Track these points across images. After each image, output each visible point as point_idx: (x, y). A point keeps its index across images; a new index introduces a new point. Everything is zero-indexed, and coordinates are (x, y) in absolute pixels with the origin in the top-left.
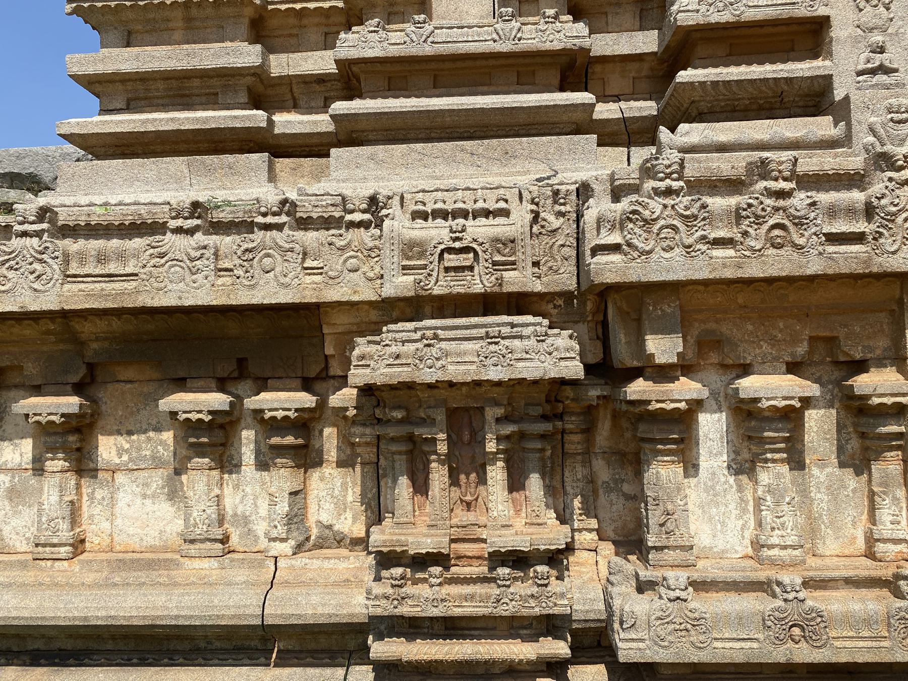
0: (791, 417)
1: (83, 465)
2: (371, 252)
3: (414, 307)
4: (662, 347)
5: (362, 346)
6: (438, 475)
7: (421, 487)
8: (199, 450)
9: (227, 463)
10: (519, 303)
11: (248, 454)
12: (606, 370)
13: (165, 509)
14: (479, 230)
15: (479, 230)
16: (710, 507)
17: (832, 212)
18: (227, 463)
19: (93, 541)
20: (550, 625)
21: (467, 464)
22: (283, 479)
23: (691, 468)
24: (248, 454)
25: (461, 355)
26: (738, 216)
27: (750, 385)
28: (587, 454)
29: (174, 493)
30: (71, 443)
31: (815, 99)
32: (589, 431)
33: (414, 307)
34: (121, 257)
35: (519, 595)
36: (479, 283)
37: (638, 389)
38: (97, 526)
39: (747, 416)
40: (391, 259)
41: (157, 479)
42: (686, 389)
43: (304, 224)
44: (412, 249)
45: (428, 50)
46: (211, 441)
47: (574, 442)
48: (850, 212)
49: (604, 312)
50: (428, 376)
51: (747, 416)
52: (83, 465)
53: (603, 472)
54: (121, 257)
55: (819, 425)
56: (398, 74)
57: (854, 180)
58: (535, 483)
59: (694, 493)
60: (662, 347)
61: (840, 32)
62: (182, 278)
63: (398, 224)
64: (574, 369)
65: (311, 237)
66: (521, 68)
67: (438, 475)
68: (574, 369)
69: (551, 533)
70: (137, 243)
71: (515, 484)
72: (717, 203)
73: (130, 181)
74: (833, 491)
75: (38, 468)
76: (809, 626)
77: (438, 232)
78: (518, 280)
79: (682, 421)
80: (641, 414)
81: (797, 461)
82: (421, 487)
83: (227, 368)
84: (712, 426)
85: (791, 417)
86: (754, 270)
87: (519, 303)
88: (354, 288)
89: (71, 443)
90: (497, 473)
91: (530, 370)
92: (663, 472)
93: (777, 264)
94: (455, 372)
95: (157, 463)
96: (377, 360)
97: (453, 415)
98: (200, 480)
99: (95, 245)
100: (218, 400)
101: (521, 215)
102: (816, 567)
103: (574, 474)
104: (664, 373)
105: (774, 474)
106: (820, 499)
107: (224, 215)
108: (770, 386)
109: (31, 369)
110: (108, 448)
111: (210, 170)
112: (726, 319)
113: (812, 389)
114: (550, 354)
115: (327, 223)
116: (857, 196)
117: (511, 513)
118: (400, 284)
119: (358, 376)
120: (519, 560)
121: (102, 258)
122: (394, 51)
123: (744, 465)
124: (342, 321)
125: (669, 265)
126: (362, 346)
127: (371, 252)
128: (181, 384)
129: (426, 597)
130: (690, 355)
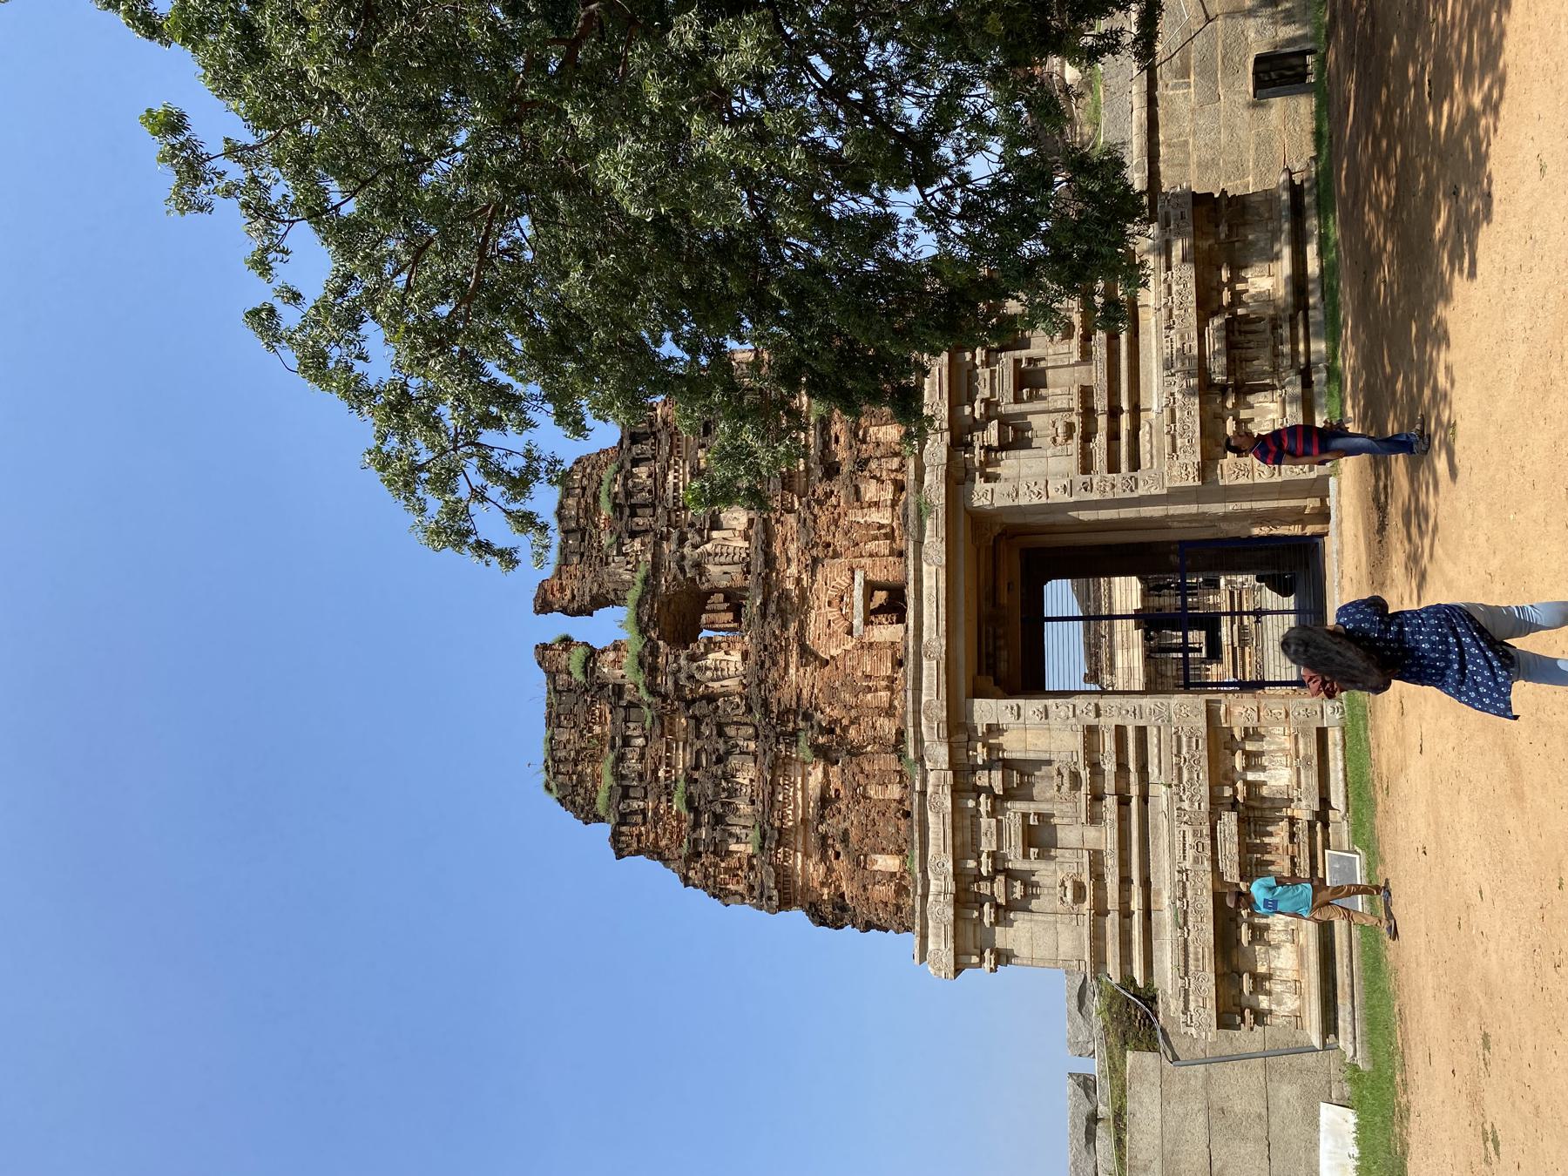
0: (1248, 755)
1: (1268, 977)
2: (1196, 874)
3: (1214, 862)
4: (1228, 792)
5: (1227, 878)
6: (1267, 857)
7: (1272, 863)
8: (1262, 936)
9: (1267, 927)
10: (1213, 829)
12: (1234, 805)
13: (1283, 950)
14: (1190, 840)
15: (1190, 840)
16: (1277, 777)
17: (1189, 746)
18: (1267, 927)
19: (1296, 977)
20: (1311, 826)
21: (1264, 848)
23: (1264, 783)
26: (1190, 772)
27: (1238, 767)
28: (1263, 809)
29: (1278, 947)
30: (1259, 980)
31: (1142, 732)
32: (1253, 808)
33: (1214, 862)
34: (1196, 953)
35: (1303, 837)
36: (1208, 842)
37: (1239, 798)
38: (1291, 975)
39: (1246, 768)
40: (1199, 867)
41: (1272, 953)
42: (1239, 785)
43: (1184, 895)
44: (1196, 860)
46: (1259, 933)
47: (1257, 813)
48: (1189, 741)
49: (1217, 805)
50: (1237, 858)
51: (1246, 768)
52: (1268, 977)
53: (1267, 805)
54: (1196, 953)
55: (1249, 747)
56: (1124, 863)
57: (1179, 738)
59: (1271, 782)
60: (1228, 792)
61: (1120, 723)
62: (1203, 933)
63: (1188, 864)
64: (1234, 815)
65: (1189, 893)
66: (1123, 819)
67: (1267, 857)
68: (1234, 815)
69: (1284, 824)
70: (1191, 949)
71: (1271, 834)
73: (1162, 962)
75: (1269, 993)
76: (1307, 759)
77: (1190, 853)
78: (1206, 830)
79: (1247, 783)
80: (1248, 797)
81: (1261, 754)
82: (1272, 863)
83: (1233, 925)
84: (1251, 776)
85: (1248, 755)
87: (1213, 829)
88: (1208, 879)
89: (1259, 980)
90: (1267, 840)
91: (1235, 829)
92: (1265, 792)
93: (1204, 763)
94: (1235, 850)
95: (1267, 952)
96: (1231, 873)
98: (1272, 937)
99: (1191, 962)
100: (1244, 928)
101: (1185, 827)
102: (1293, 752)
103: (1267, 814)
104: (1235, 791)
105: (1265, 761)
106: (1273, 747)
107: (1181, 921)
108: (1239, 761)
109: (1234, 992)
110: (1262, 969)
111: (1158, 933)
112: (1220, 775)
113: (1239, 753)
115: (1184, 888)
116: (1184, 739)
117: (1278, 836)
118: (1207, 865)
119: (1236, 879)
120: (1292, 836)
121: (1197, 960)
123: (1264, 769)
124: (1218, 886)
125: (1205, 790)
126: (1227, 878)
127: (1196, 874)
128: (1239, 941)
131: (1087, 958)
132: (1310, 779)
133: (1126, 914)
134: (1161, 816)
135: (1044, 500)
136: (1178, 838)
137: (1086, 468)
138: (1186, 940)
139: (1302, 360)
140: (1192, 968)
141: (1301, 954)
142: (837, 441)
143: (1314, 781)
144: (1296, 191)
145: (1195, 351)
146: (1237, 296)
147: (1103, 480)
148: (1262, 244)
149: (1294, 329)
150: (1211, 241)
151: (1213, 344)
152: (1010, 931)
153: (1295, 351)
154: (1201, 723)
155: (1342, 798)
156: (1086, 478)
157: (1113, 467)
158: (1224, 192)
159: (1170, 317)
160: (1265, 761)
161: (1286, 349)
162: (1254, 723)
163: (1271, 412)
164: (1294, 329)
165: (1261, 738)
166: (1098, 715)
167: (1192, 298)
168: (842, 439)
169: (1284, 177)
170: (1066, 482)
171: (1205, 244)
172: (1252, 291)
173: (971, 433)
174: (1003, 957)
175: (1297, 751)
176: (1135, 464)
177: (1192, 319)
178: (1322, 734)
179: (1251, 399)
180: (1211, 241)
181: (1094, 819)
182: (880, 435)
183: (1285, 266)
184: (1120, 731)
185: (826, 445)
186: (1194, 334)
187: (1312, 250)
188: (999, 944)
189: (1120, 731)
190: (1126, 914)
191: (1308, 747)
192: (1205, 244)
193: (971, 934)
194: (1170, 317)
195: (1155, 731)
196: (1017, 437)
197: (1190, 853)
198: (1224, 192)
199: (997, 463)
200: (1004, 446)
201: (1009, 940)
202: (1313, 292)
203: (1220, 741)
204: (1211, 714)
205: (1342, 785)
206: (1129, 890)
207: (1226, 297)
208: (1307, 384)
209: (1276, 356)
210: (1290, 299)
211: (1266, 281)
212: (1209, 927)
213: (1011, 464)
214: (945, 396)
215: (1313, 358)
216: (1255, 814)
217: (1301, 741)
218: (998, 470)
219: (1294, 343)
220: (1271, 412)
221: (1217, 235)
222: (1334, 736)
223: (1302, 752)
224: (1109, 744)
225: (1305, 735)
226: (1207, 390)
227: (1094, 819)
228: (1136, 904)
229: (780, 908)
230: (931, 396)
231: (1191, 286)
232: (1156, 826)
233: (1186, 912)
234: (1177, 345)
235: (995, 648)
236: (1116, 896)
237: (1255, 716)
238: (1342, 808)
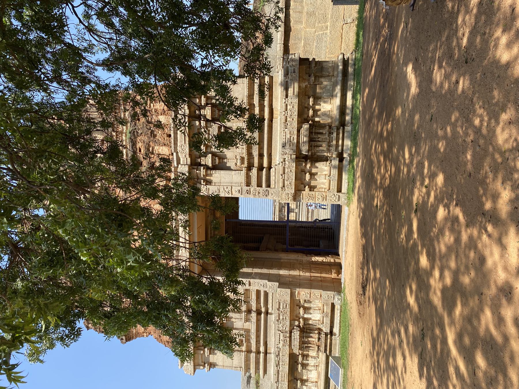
1: (307, 381)
4: (297, 323)
6: (309, 345)
9: (307, 365)
11: (307, 362)
14: (282, 338)
15: (282, 338)
16: (315, 317)
18: (307, 365)
22: (310, 359)
23: (310, 319)
24: (307, 362)
25: (296, 343)
29: (311, 371)
36: (288, 339)
42: (301, 320)
44: (283, 345)
45: (255, 334)
48: (283, 305)
52: (307, 381)
54: (282, 375)
55: (306, 305)
56: (258, 337)
57: (279, 303)
58: (311, 335)
62: (285, 369)
63: (280, 346)
65: (281, 354)
66: (258, 321)
70: (280, 373)
71: (311, 337)
72: (281, 318)
74: (314, 304)
77: (282, 342)
78: (288, 335)
79: (305, 320)
83: (296, 364)
84: (306, 316)
86: (289, 315)
90: (310, 339)
92: (310, 322)
93: (288, 313)
94: (298, 344)
95: (307, 372)
97: (303, 344)
99: (280, 377)
100: (300, 365)
106: (315, 306)
109: (294, 385)
110: (305, 378)
111: (269, 361)
112: (294, 317)
114: (296, 334)
116: (281, 304)
117: (314, 338)
118: (287, 347)
120: (319, 339)
122: (255, 338)
123: (311, 314)
125: (288, 323)
128: (297, 369)
129: (322, 348)
130: (297, 319)
131: (243, 367)
132: (327, 321)
133: (258, 352)
134: (272, 323)
135: (230, 196)
136: (278, 337)
137: (248, 184)
138: (278, 371)
139: (340, 148)
140: (280, 380)
141: (319, 374)
142: (140, 151)
143: (329, 322)
144: (345, 63)
145: (295, 141)
146: (315, 111)
147: (255, 190)
148: (328, 87)
149: (338, 134)
150: (307, 83)
151: (304, 139)
152: (216, 356)
153: (337, 146)
154: (288, 299)
155: (338, 329)
156: (248, 188)
157: (259, 185)
158: (314, 59)
159: (286, 121)
160: (311, 311)
161: (334, 142)
162: (309, 298)
163: (325, 171)
164: (338, 134)
165: (311, 302)
166: (250, 285)
167: (296, 113)
168: (142, 151)
169: (341, 57)
170: (239, 188)
171: (304, 85)
172: (322, 110)
173: (200, 157)
174: (212, 365)
175: (323, 309)
176: (268, 185)
177: (295, 124)
178: (333, 306)
179: (317, 164)
180: (307, 83)
181: (247, 320)
182: (160, 151)
183: (337, 101)
184: (258, 292)
185: (135, 152)
186: (296, 132)
187: (349, 95)
188: (211, 360)
189: (258, 292)
190: (258, 352)
191: (328, 309)
192: (304, 85)
193: (200, 358)
194: (286, 121)
195: (271, 294)
196: (220, 165)
197: (282, 342)
198: (314, 59)
199: (211, 175)
200: (215, 167)
201: (215, 359)
202: (348, 114)
203: (295, 304)
204: (292, 295)
205: (338, 325)
206: (260, 343)
207: (311, 112)
208: (341, 159)
209: (329, 146)
210: (338, 117)
211: (329, 107)
212: (287, 367)
213: (217, 176)
214: (187, 142)
215: (344, 148)
216: (306, 330)
217: (325, 307)
218: (212, 178)
219: (337, 141)
220: (325, 171)
221: (309, 80)
222: (337, 307)
223: (325, 311)
224: (254, 296)
225: (327, 305)
226: (300, 158)
227: (247, 320)
228: (262, 349)
229: (127, 341)
230: (181, 141)
231: (296, 107)
232: (270, 326)
233: (279, 361)
234: (288, 136)
235: (214, 235)
236: (255, 346)
237: (309, 296)
238: (337, 333)
